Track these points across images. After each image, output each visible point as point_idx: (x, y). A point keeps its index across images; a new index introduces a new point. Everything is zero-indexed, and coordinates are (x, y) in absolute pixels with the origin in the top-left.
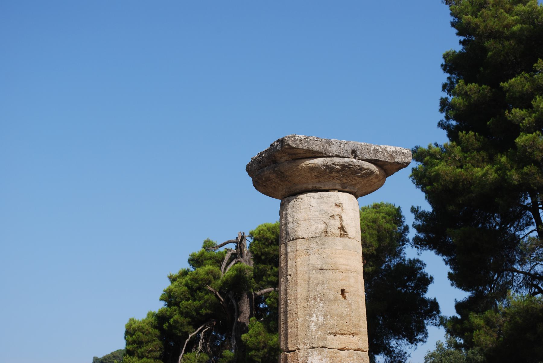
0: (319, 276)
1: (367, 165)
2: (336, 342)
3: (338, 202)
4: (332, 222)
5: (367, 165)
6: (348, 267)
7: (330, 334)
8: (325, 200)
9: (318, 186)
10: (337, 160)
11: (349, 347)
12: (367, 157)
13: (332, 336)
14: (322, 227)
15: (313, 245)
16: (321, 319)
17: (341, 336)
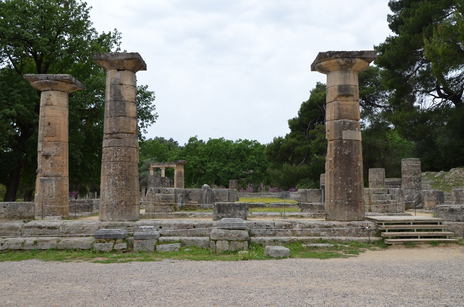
0: (43, 119)
1: (53, 81)
2: (46, 139)
3: (50, 94)
4: (49, 101)
5: (53, 81)
6: (51, 115)
7: (44, 137)
8: (46, 94)
9: (45, 89)
10: (42, 81)
11: (51, 141)
12: (52, 79)
13: (45, 137)
14: (45, 103)
15: (42, 109)
16: (42, 132)
17: (48, 137)
